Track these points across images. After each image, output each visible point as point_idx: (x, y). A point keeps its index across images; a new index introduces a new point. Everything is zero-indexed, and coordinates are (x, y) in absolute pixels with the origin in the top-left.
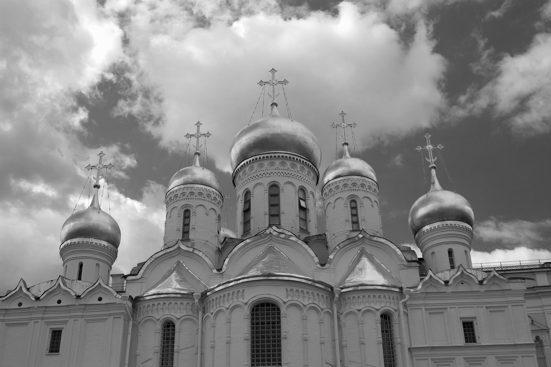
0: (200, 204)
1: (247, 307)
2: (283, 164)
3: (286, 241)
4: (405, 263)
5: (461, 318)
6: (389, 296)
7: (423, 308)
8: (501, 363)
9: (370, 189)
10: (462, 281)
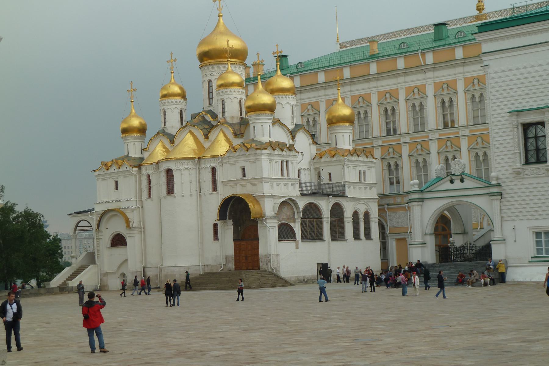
1: (163, 171)
2: (213, 68)
4: (234, 136)
5: (240, 167)
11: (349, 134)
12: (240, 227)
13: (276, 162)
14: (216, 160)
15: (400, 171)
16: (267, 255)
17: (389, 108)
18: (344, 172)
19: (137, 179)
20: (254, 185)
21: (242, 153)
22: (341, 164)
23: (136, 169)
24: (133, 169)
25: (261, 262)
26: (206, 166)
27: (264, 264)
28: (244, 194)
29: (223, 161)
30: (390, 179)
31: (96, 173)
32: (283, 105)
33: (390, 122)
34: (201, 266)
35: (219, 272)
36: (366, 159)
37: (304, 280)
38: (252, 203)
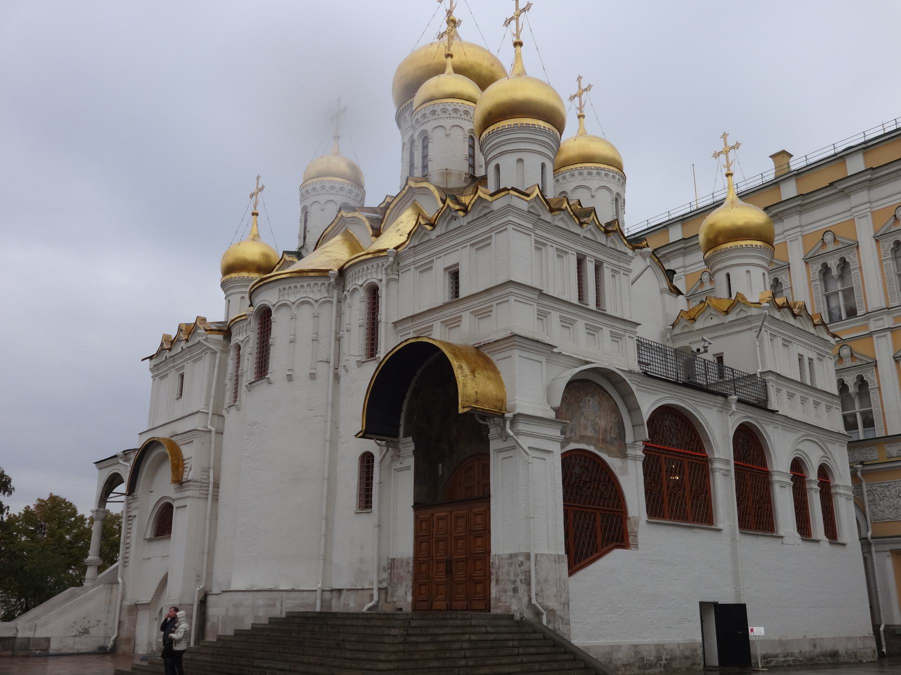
0: (313, 202)
3: (355, 219)
5: (446, 269)
6: (378, 264)
7: (412, 267)
8: (479, 319)
9: (446, 112)
10: (453, 216)
11: (762, 271)
12: (440, 465)
13: (561, 253)
14: (380, 264)
15: (874, 395)
16: (516, 555)
17: (833, 264)
18: (761, 347)
19: (217, 360)
20: (483, 314)
21: (454, 225)
22: (750, 329)
23: (220, 337)
24: (209, 336)
25: (497, 581)
26: (352, 289)
27: (505, 591)
28: (448, 345)
29: (401, 265)
30: (845, 417)
31: (154, 362)
32: (591, 192)
33: (837, 293)
34: (319, 592)
35: (363, 614)
36: (812, 330)
37: (659, 658)
38: (468, 363)
